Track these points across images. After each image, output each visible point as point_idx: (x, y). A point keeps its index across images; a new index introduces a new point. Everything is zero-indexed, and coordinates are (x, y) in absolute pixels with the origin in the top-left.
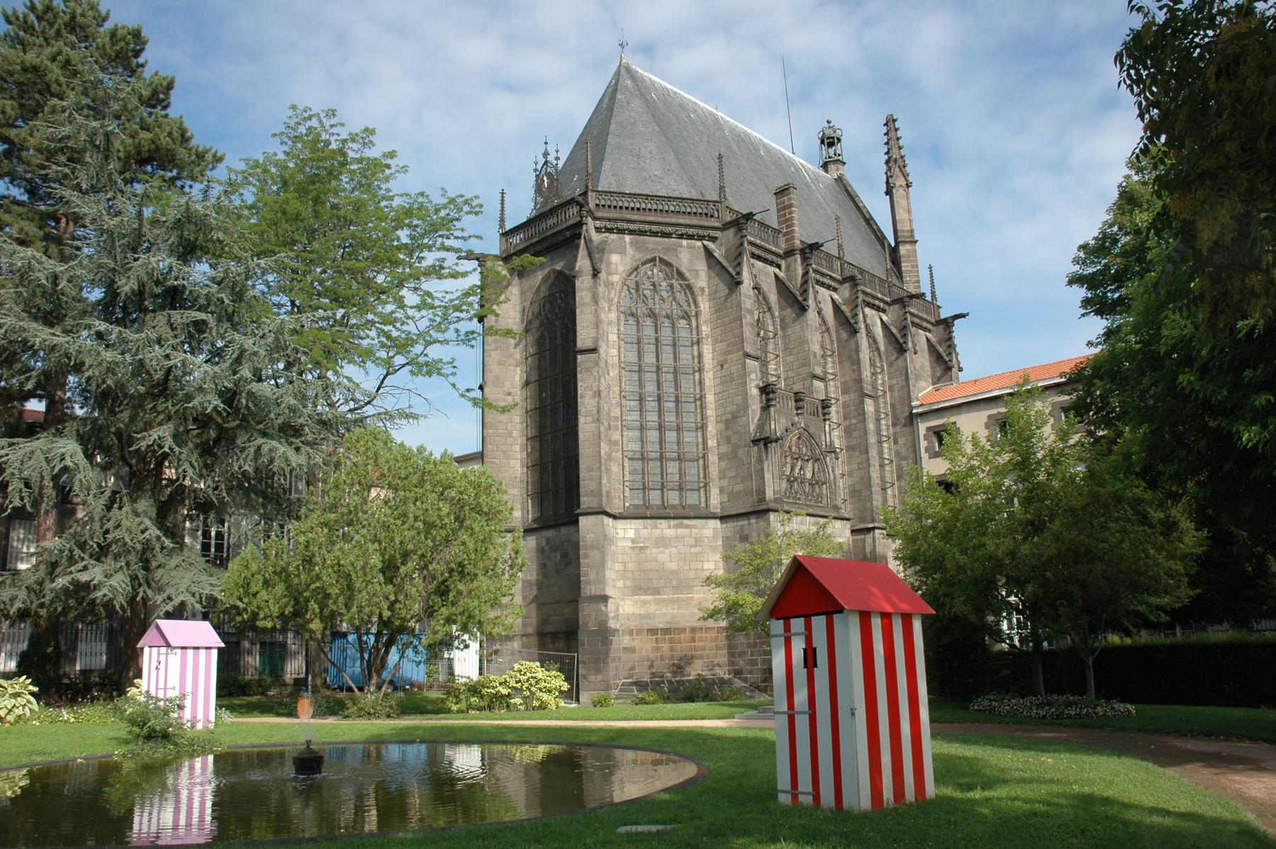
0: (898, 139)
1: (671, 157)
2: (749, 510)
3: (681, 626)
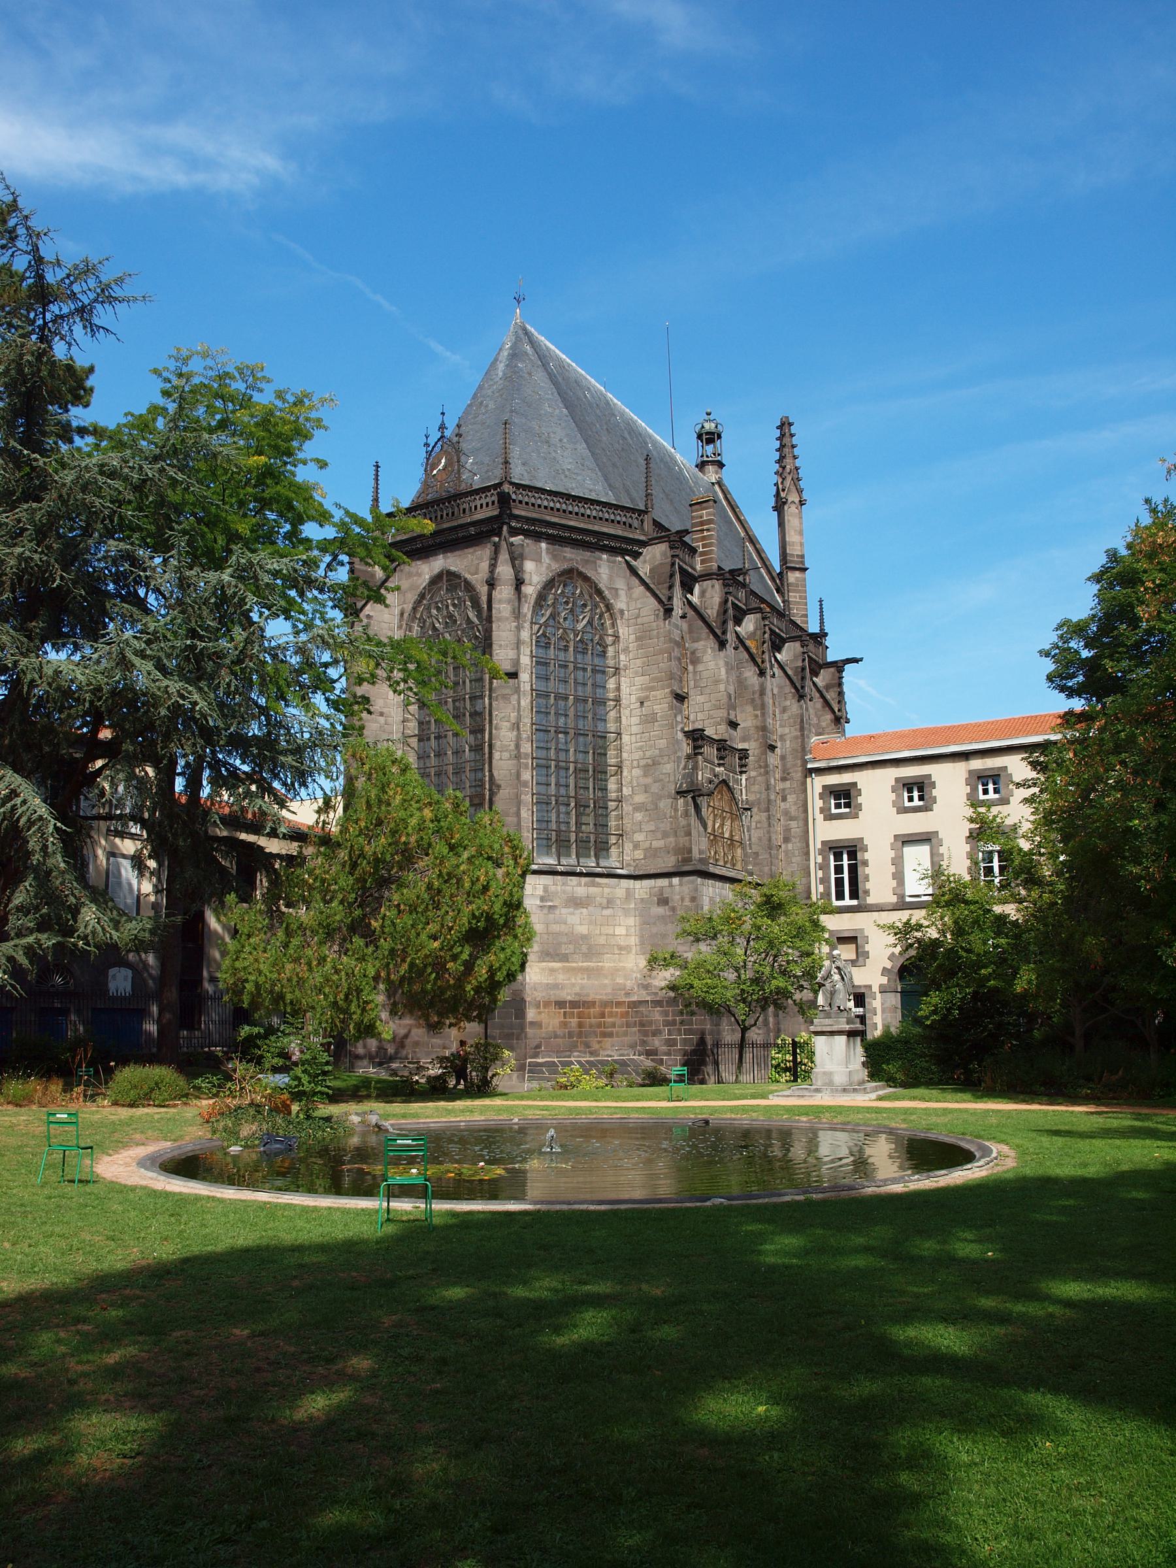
0: (793, 447)
1: (582, 447)
2: (672, 870)
3: (590, 999)
